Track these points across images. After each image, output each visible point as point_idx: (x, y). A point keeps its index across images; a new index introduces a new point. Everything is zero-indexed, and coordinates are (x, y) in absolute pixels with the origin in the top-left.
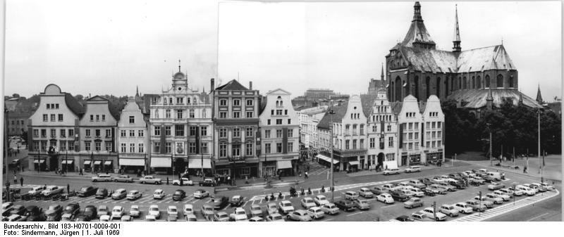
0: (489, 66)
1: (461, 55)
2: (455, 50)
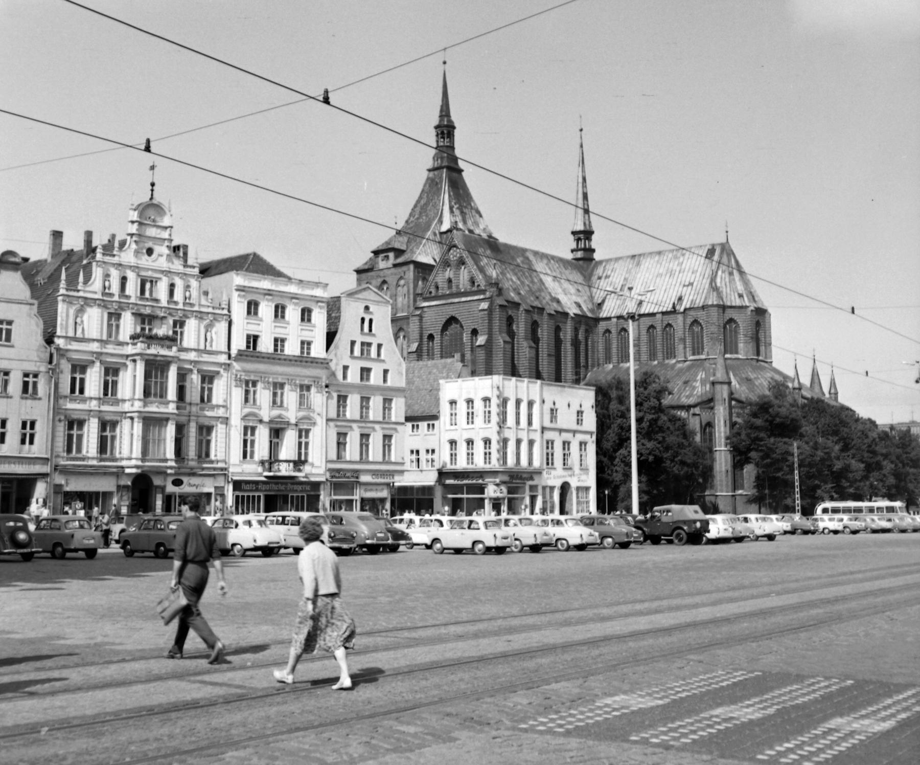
0: (696, 297)
1: (599, 271)
2: (579, 254)
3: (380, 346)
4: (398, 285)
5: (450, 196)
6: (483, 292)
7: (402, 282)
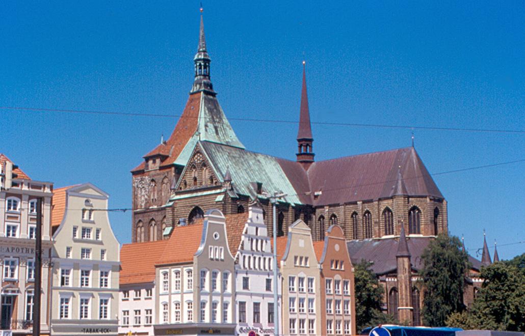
3: (98, 231)
4: (163, 183)
5: (205, 113)
6: (220, 187)
7: (166, 181)
